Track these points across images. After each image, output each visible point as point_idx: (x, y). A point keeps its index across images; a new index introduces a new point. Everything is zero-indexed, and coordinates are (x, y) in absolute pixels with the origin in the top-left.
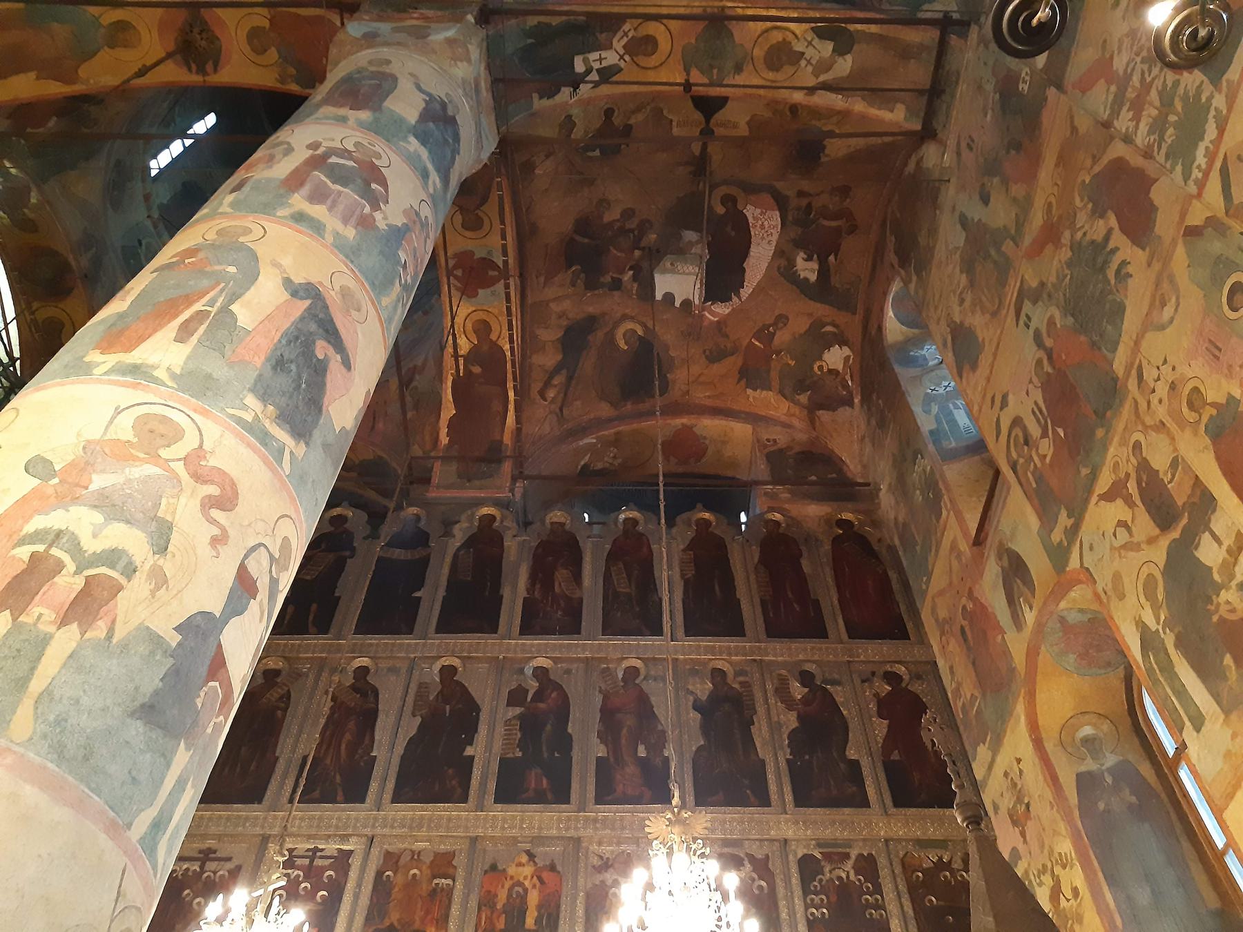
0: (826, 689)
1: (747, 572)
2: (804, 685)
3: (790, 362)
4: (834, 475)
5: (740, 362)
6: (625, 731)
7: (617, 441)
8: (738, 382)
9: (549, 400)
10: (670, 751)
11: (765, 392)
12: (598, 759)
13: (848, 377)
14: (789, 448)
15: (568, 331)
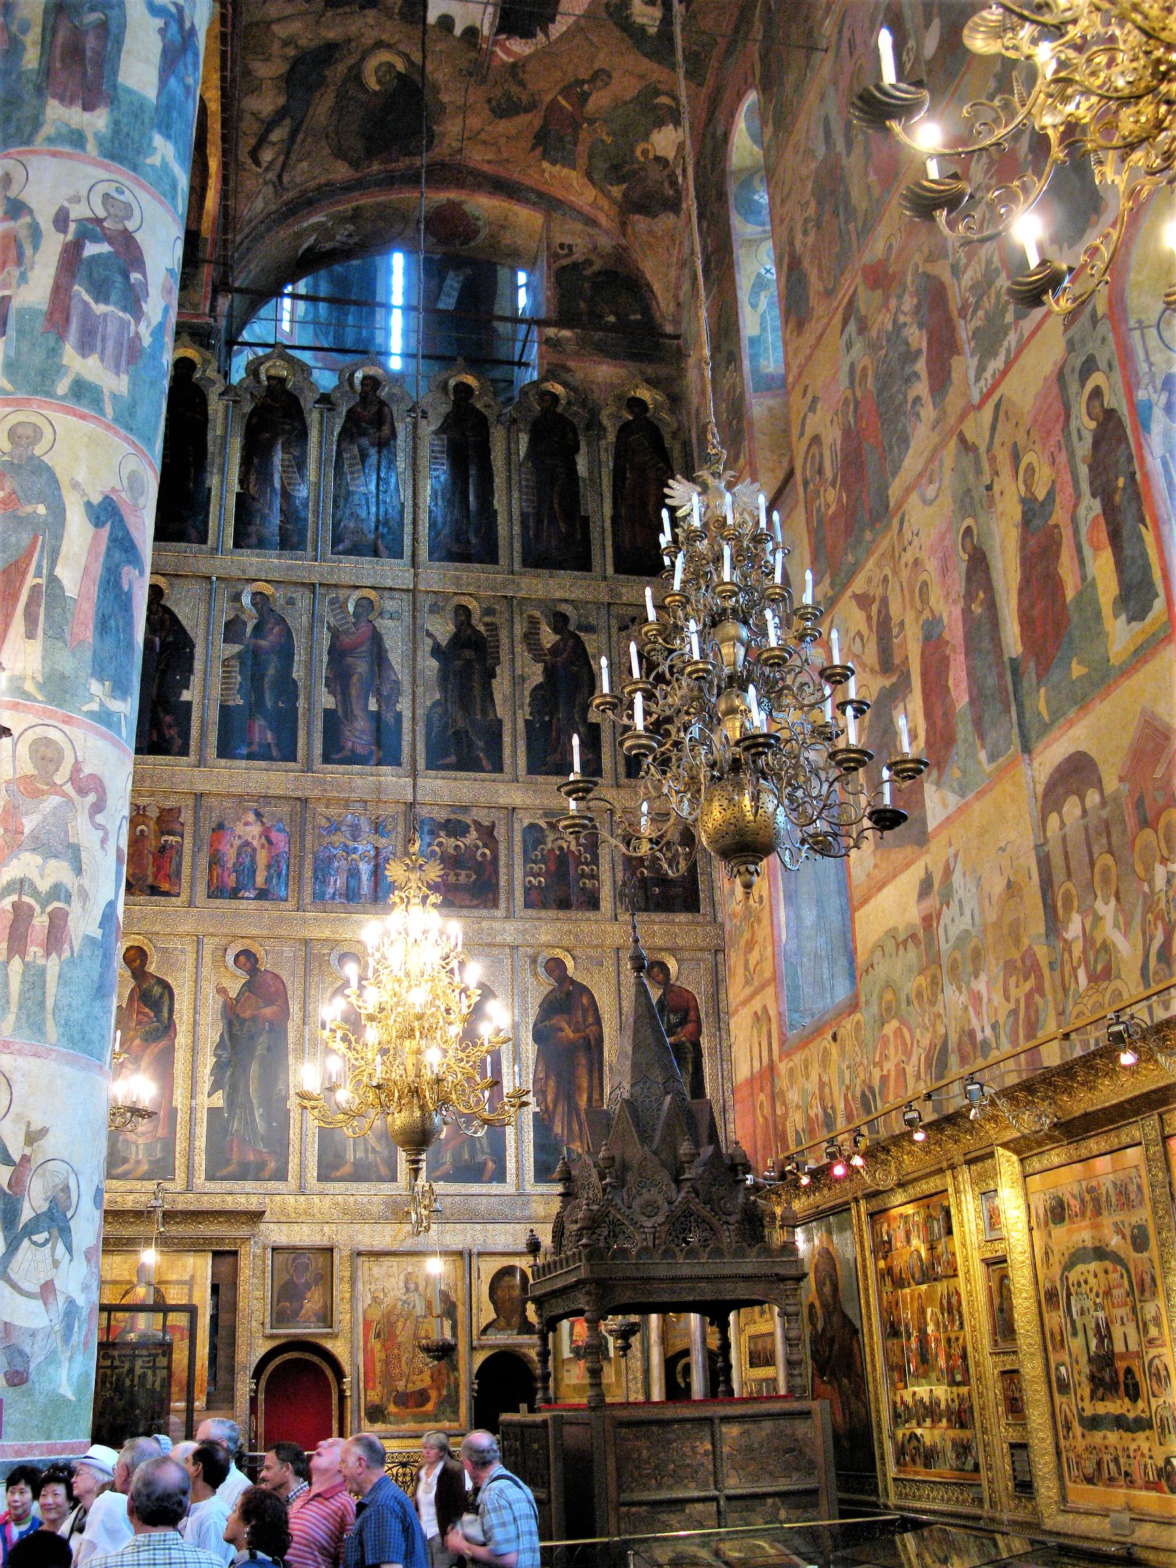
0: (578, 637)
1: (509, 471)
2: (556, 630)
3: (605, 138)
4: (639, 317)
5: (538, 123)
6: (355, 679)
7: (356, 215)
8: (533, 149)
9: (265, 165)
10: (404, 705)
11: (566, 171)
12: (326, 711)
13: (679, 171)
14: (588, 262)
15: (296, 63)
